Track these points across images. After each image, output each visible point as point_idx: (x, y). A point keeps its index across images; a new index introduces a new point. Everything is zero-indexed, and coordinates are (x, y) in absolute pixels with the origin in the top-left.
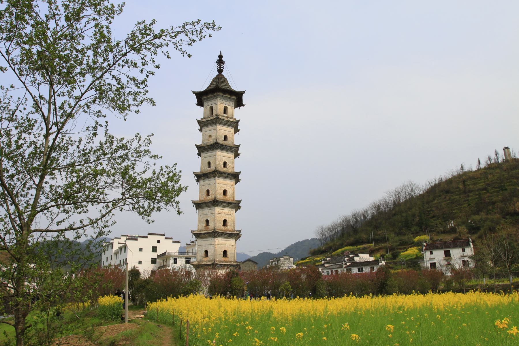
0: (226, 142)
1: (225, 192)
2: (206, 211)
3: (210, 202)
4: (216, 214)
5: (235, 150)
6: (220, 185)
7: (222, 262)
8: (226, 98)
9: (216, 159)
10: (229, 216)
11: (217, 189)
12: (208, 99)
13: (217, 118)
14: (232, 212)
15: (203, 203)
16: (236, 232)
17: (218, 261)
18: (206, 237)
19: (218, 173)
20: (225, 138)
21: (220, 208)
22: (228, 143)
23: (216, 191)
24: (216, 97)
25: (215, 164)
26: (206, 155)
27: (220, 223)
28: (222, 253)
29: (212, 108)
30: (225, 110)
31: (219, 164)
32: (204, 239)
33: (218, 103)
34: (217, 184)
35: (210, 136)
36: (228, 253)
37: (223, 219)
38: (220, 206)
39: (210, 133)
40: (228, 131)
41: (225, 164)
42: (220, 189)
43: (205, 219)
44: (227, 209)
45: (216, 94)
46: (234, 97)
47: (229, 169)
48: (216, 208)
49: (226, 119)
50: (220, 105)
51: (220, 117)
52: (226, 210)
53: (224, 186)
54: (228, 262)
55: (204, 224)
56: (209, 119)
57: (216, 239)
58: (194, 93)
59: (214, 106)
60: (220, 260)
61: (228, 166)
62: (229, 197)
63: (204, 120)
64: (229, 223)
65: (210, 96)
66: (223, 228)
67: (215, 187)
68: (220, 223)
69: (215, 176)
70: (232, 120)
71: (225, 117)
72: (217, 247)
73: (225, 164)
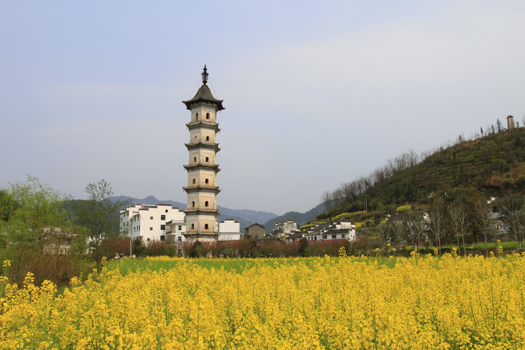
0: (208, 142)
1: (207, 181)
2: (193, 195)
4: (200, 197)
5: (216, 148)
7: (204, 232)
8: (208, 107)
9: (200, 155)
12: (194, 107)
13: (201, 123)
16: (214, 211)
17: (201, 232)
18: (193, 215)
20: (208, 138)
22: (210, 142)
23: (199, 180)
24: (200, 106)
25: (199, 159)
27: (203, 204)
29: (197, 114)
30: (208, 116)
33: (202, 111)
34: (201, 175)
38: (203, 191)
39: (196, 134)
40: (210, 133)
41: (207, 159)
46: (215, 105)
47: (210, 163)
48: (200, 193)
49: (208, 124)
50: (203, 112)
51: (203, 122)
52: (207, 194)
55: (191, 205)
56: (195, 124)
57: (199, 216)
58: (183, 102)
59: (199, 113)
61: (209, 160)
62: (210, 184)
63: (191, 124)
64: (209, 204)
65: (196, 104)
66: (205, 207)
68: (203, 204)
69: (199, 169)
70: (212, 124)
72: (200, 222)
73: (207, 159)
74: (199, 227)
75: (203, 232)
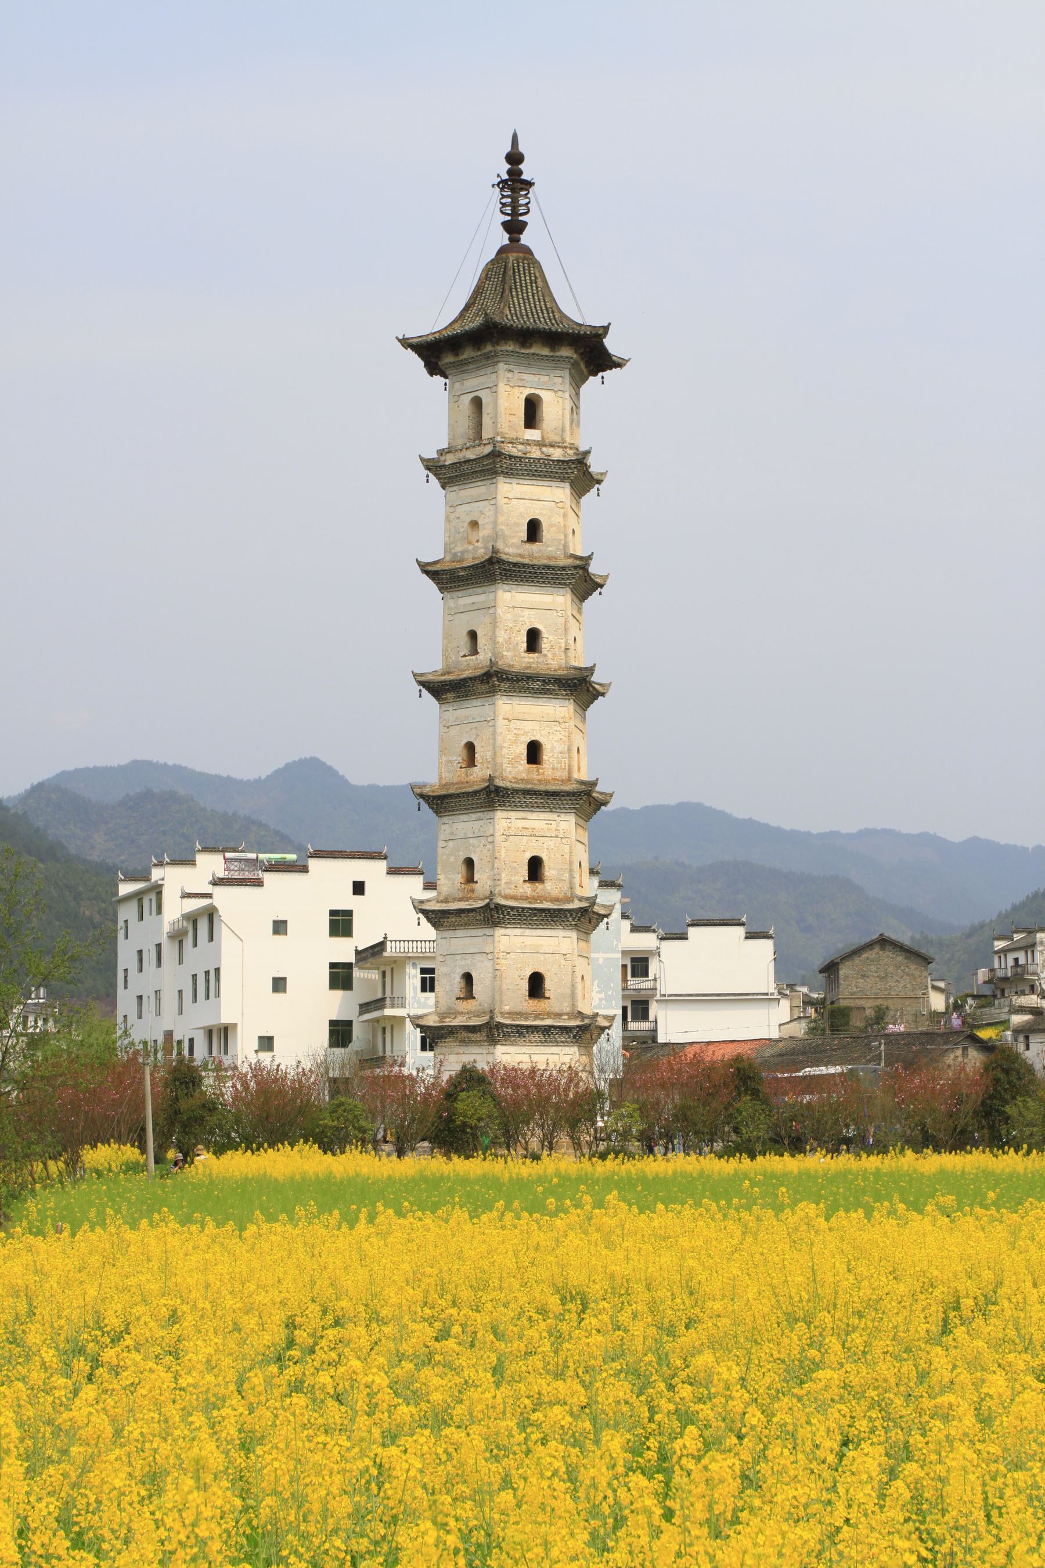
0: (535, 547)
4: (499, 838)
6: (513, 725)
10: (551, 843)
11: (499, 740)
14: (563, 825)
17: (511, 1014)
21: (513, 815)
24: (491, 359)
34: (501, 723)
37: (528, 855)
38: (515, 807)
42: (515, 742)
44: (542, 816)
48: (499, 815)
53: (528, 726)
57: (499, 932)
60: (518, 1008)
66: (528, 889)
69: (493, 691)
75: (520, 1014)
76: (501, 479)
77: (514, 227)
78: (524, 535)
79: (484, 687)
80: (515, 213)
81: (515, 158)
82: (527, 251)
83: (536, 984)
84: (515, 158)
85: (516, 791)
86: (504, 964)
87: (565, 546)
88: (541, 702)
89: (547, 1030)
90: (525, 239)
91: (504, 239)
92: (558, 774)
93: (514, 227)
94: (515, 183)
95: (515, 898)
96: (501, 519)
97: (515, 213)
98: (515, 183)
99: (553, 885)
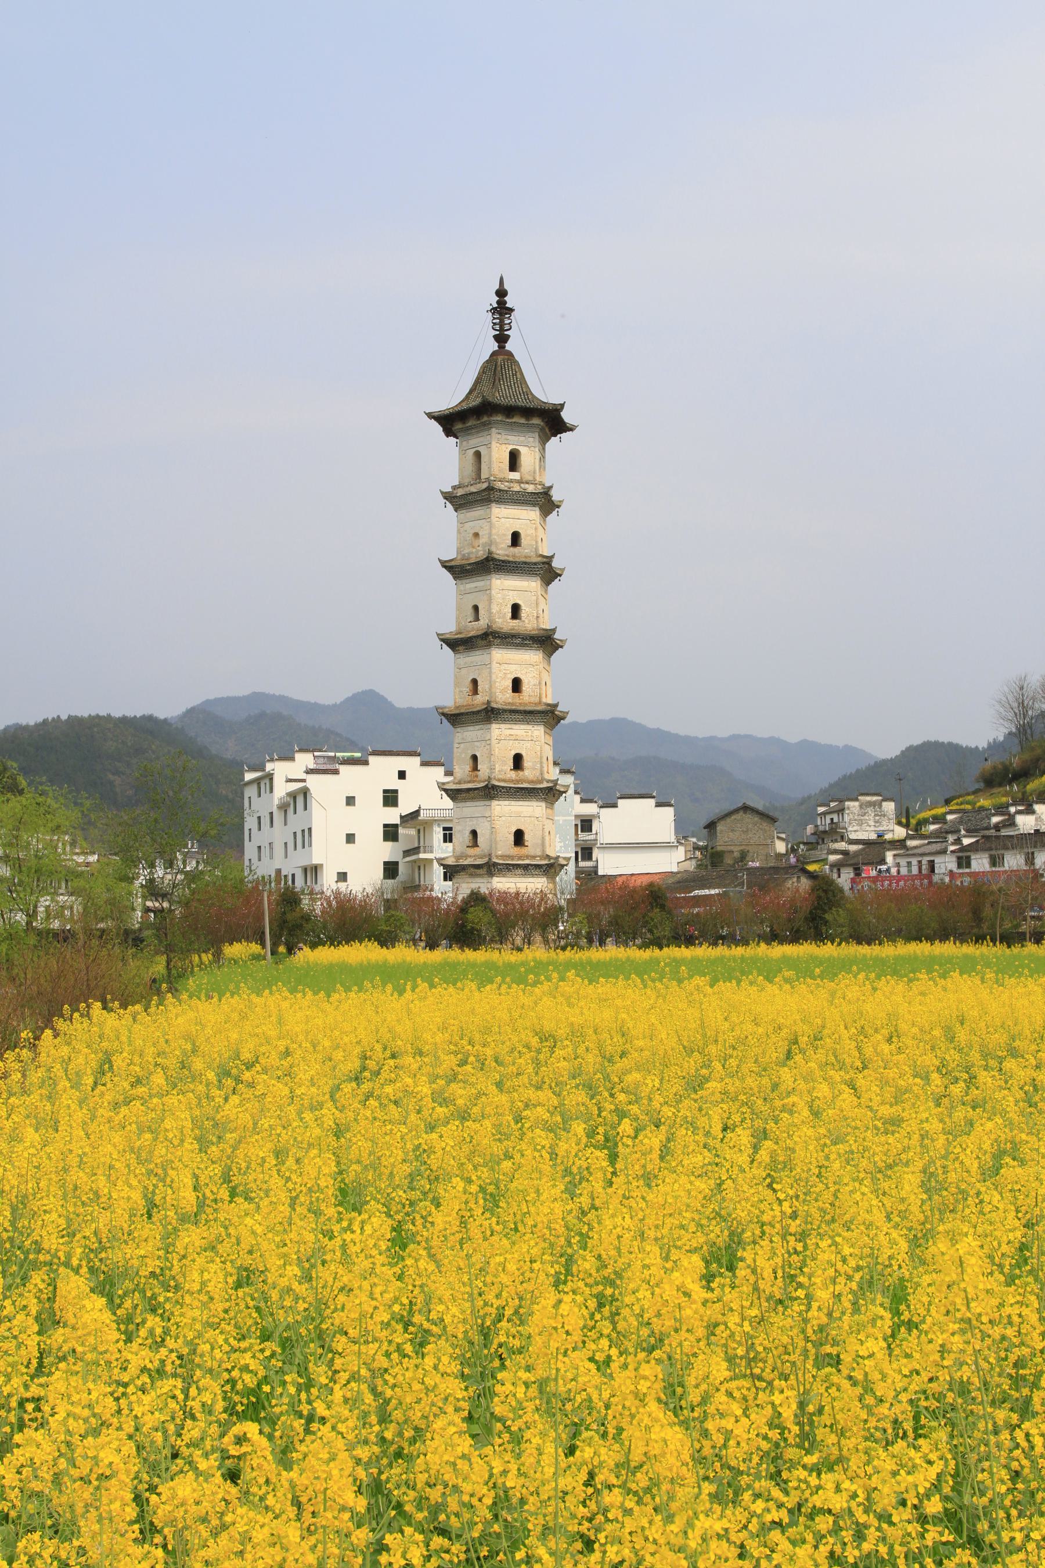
0: (516, 550)
3: (479, 712)
4: (494, 742)
7: (512, 857)
9: (490, 600)
10: (528, 744)
15: (462, 714)
17: (503, 857)
18: (473, 799)
19: (495, 637)
24: (487, 426)
26: (468, 586)
28: (512, 838)
31: (499, 612)
32: (468, 804)
34: (494, 665)
35: (476, 535)
36: (526, 837)
37: (513, 753)
38: (505, 721)
43: (470, 753)
44: (522, 727)
45: (485, 419)
52: (520, 730)
53: (513, 668)
54: (527, 857)
59: (483, 451)
60: (508, 853)
65: (471, 423)
66: (513, 775)
67: (490, 673)
69: (489, 645)
71: (511, 481)
74: (493, 841)
76: (493, 505)
77: (502, 339)
78: (509, 542)
79: (484, 642)
80: (502, 329)
81: (501, 293)
82: (510, 354)
83: (519, 837)
84: (501, 293)
85: (505, 711)
86: (498, 824)
87: (536, 549)
88: (521, 652)
89: (526, 867)
90: (509, 346)
91: (495, 346)
92: (532, 700)
93: (502, 339)
94: (502, 310)
95: (504, 781)
96: (494, 531)
97: (502, 329)
98: (502, 310)
99: (530, 771)
